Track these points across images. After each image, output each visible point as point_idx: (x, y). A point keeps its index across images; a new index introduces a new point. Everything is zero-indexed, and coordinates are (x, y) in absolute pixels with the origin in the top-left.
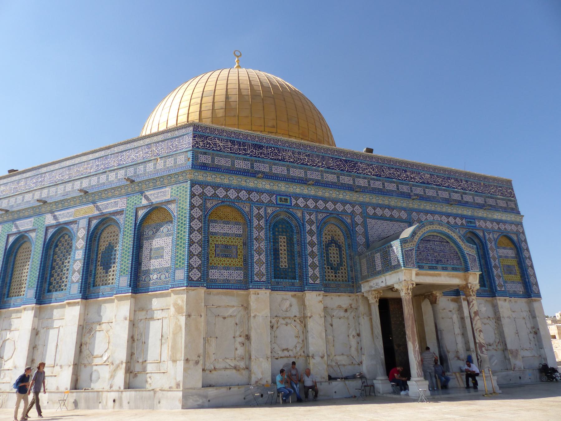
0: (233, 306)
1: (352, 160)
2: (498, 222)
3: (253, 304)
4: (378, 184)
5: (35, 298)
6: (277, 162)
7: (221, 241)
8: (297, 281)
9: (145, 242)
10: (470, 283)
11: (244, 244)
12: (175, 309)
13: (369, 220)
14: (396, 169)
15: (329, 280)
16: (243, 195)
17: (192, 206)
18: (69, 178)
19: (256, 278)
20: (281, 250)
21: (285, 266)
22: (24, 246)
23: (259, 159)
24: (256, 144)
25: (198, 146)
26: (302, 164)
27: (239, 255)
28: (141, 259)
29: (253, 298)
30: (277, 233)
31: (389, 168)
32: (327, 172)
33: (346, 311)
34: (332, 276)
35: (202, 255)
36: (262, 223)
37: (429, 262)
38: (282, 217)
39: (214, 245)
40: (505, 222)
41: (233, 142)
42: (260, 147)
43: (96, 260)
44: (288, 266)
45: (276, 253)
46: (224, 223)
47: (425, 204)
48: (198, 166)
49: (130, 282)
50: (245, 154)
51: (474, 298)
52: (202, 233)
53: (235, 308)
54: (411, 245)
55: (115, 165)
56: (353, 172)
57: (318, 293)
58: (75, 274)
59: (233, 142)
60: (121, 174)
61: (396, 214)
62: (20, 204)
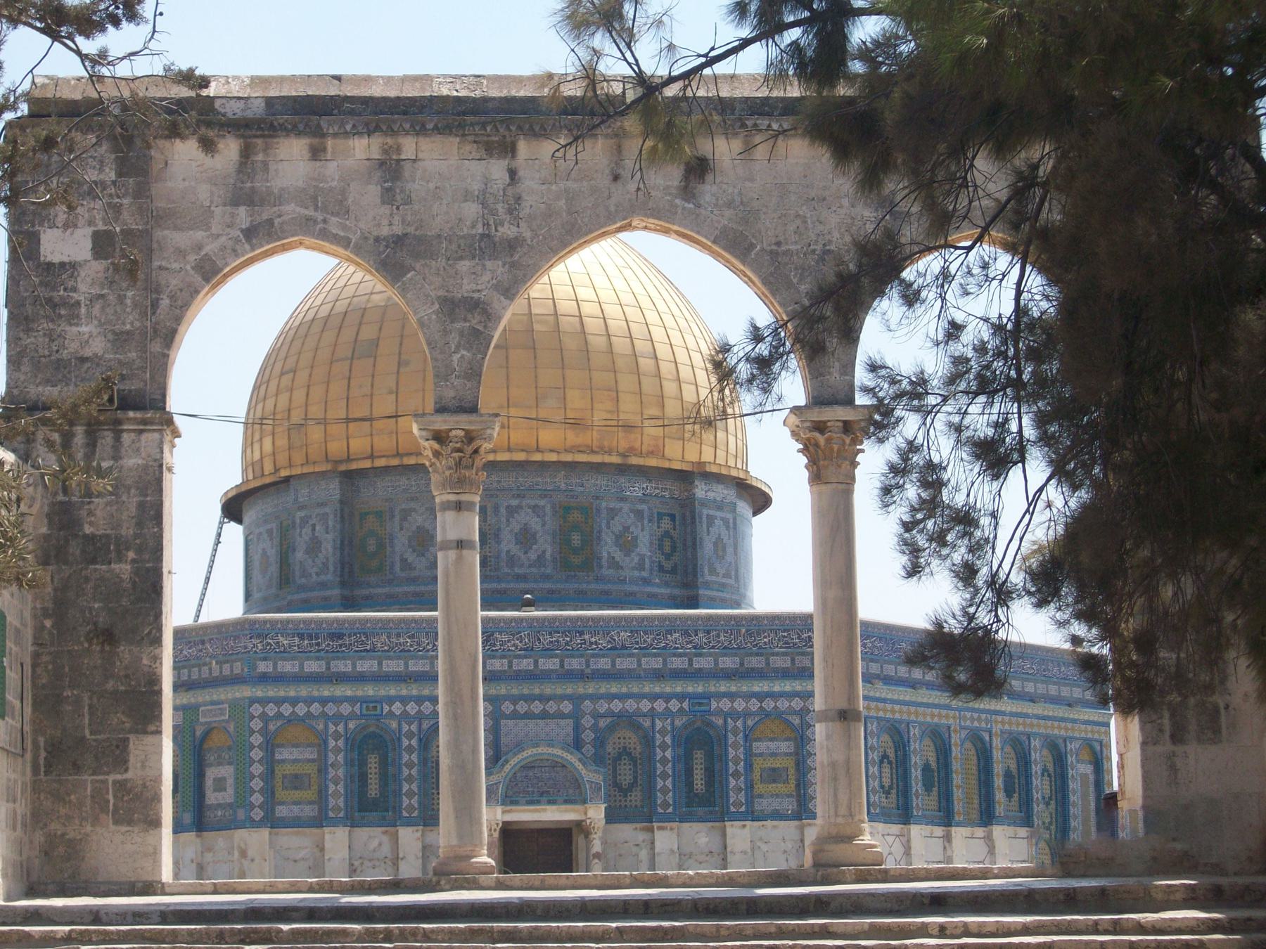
0: (306, 848)
2: (761, 697)
3: (328, 845)
4: (526, 664)
7: (289, 769)
11: (319, 771)
13: (503, 722)
19: (331, 814)
23: (338, 654)
29: (327, 837)
36: (341, 743)
38: (372, 729)
40: (773, 696)
41: (301, 637)
42: (340, 636)
45: (363, 778)
46: (293, 746)
50: (319, 651)
57: (415, 828)
61: (552, 707)
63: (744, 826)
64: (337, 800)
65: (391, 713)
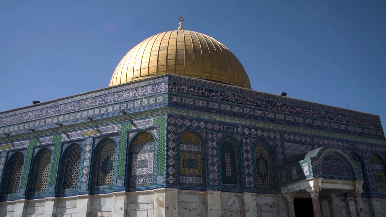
0: (196, 202)
1: (273, 101)
2: (372, 145)
3: (210, 201)
4: (291, 118)
5: (55, 192)
6: (224, 101)
8: (238, 185)
9: (134, 155)
10: (357, 188)
11: (203, 159)
12: (158, 203)
14: (302, 107)
15: (259, 185)
16: (202, 124)
17: (169, 132)
18: (79, 109)
19: (211, 183)
20: (227, 163)
21: (230, 175)
22: (45, 155)
24: (209, 89)
25: (172, 90)
26: (240, 103)
27: (199, 167)
28: (132, 168)
29: (209, 197)
30: (224, 151)
31: (298, 107)
32: (257, 109)
33: (271, 206)
34: (261, 182)
35: (175, 166)
36: (214, 144)
37: (329, 174)
38: (227, 140)
39: (183, 159)
40: (376, 146)
41: (194, 88)
42: (213, 91)
43: (98, 168)
44: (232, 174)
45: (223, 165)
46: (189, 144)
47: (322, 133)
48: (172, 104)
49: (125, 183)
50: (203, 96)
51: (360, 199)
52: (175, 151)
53: (197, 203)
54: (318, 162)
55: (113, 101)
56: (274, 109)
58: (84, 177)
59: (194, 88)
60: (117, 107)
61: (303, 139)
62: (43, 125)
63: (377, 200)
64: (214, 176)
65: (237, 132)
